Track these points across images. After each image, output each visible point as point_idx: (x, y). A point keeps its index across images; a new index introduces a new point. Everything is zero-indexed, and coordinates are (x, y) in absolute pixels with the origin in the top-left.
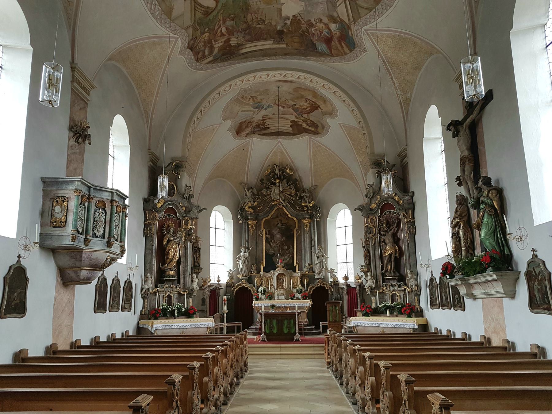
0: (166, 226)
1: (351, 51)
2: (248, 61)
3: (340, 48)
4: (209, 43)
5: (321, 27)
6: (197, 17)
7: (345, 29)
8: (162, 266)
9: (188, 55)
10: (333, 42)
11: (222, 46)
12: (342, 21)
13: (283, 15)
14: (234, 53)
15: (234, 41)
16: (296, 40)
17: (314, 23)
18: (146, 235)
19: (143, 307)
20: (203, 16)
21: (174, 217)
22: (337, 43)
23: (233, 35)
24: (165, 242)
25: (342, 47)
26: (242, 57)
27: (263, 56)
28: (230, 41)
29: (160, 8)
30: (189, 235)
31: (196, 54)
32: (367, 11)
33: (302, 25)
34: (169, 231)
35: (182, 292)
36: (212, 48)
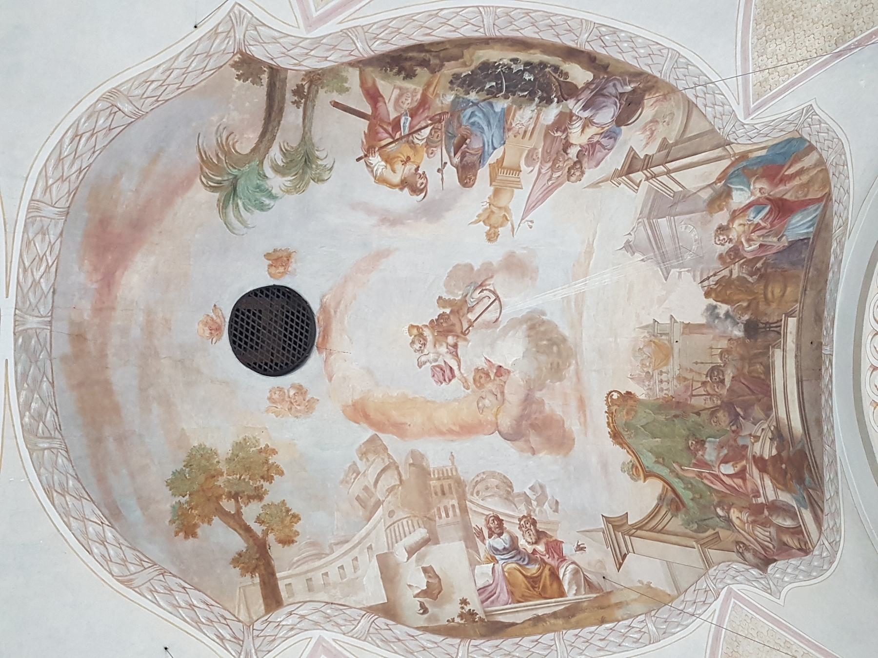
1: (811, 148)
2: (830, 419)
3: (805, 178)
4: (760, 512)
5: (741, 228)
6: (682, 529)
7: (744, 168)
9: (784, 572)
10: (786, 197)
11: (773, 479)
12: (725, 176)
13: (703, 321)
14: (802, 454)
15: (762, 447)
16: (777, 291)
17: (729, 245)
20: (681, 516)
22: (788, 186)
23: (745, 447)
25: (801, 172)
26: (814, 433)
27: (819, 377)
28: (762, 458)
29: (642, 618)
31: (784, 550)
32: (695, 115)
33: (735, 275)
36: (775, 507)
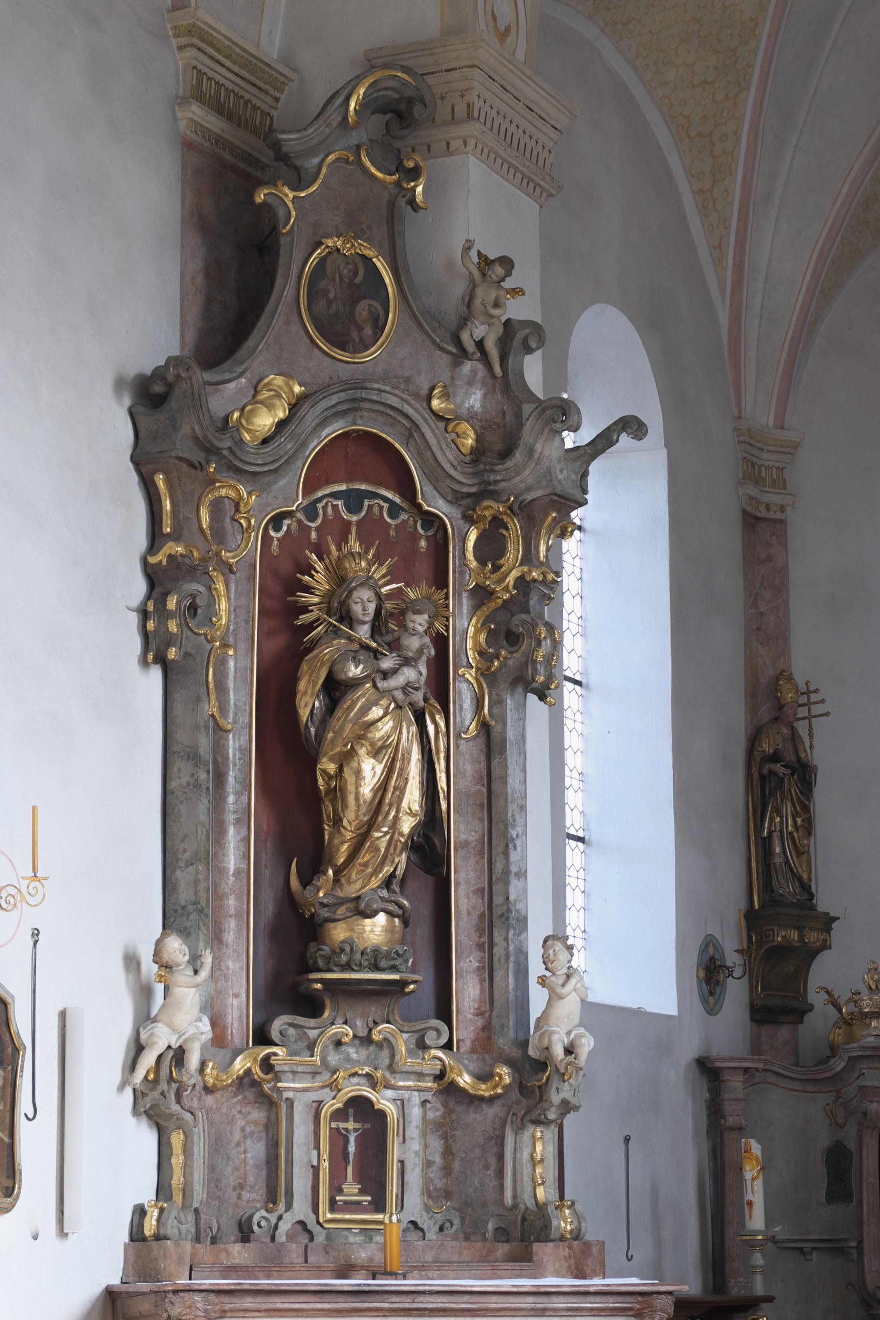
0: (320, 580)
8: (306, 881)
18: (154, 649)
19: (163, 1190)
21: (394, 510)
24: (308, 702)
30: (512, 638)
34: (348, 618)
35: (465, 1080)
